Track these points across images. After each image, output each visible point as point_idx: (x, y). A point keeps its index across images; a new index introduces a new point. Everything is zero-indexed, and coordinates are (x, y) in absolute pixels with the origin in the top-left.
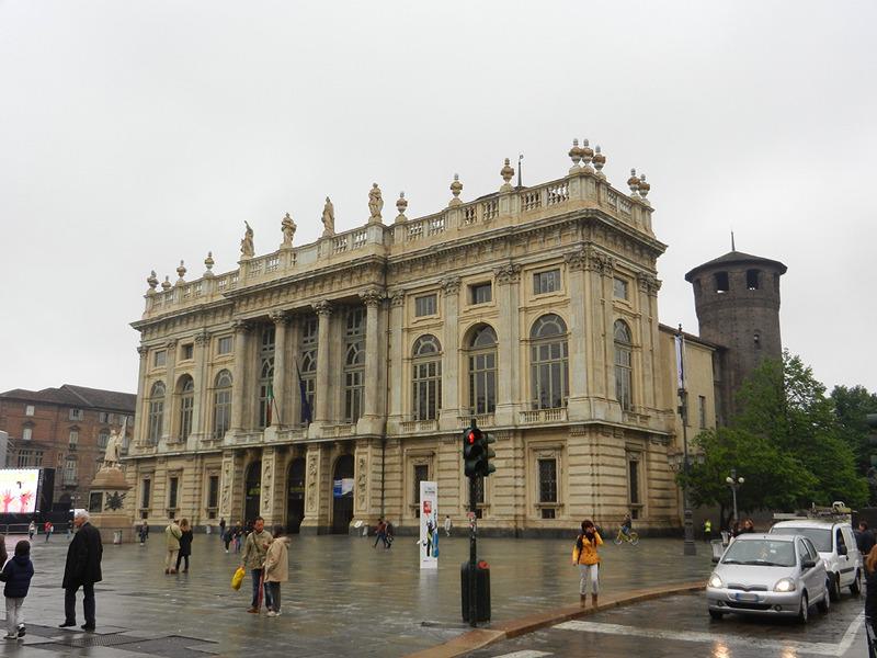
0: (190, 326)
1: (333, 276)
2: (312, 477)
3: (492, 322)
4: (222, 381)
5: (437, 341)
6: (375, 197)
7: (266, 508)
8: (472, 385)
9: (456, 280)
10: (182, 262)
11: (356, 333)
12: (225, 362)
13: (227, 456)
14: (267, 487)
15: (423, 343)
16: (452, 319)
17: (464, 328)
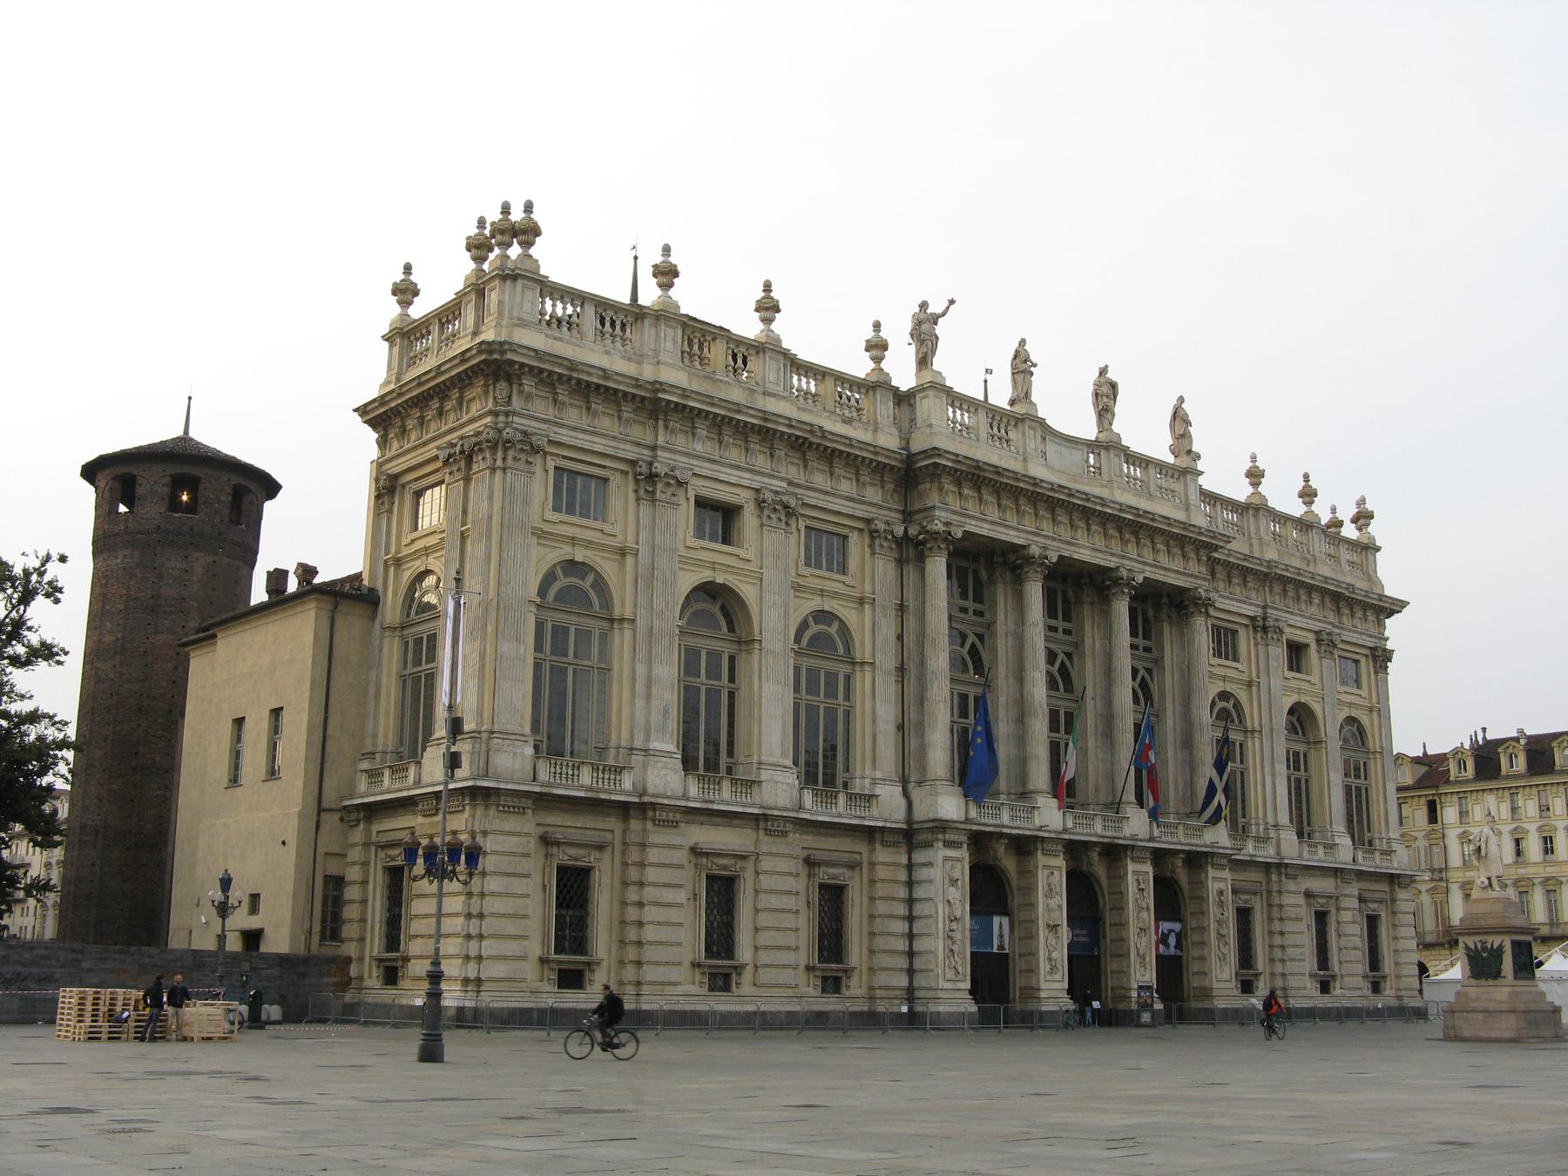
0: (734, 454)
1: (1153, 532)
2: (1145, 914)
3: (1317, 708)
4: (822, 639)
5: (1238, 706)
6: (1179, 419)
7: (1053, 970)
8: (731, 715)
9: (1281, 624)
10: (667, 250)
11: (1147, 649)
12: (835, 595)
13: (949, 844)
14: (1054, 928)
15: (1221, 705)
16: (1276, 684)
17: (1288, 702)
